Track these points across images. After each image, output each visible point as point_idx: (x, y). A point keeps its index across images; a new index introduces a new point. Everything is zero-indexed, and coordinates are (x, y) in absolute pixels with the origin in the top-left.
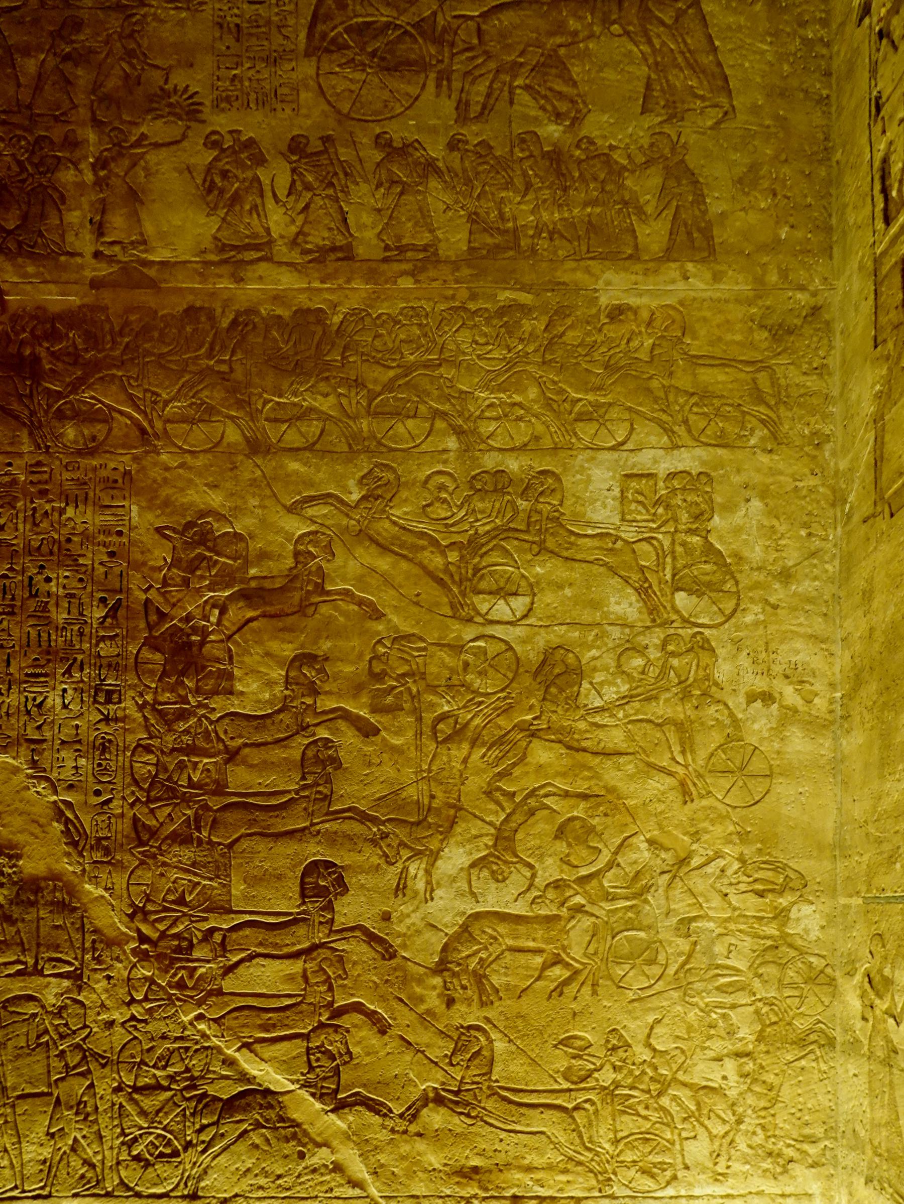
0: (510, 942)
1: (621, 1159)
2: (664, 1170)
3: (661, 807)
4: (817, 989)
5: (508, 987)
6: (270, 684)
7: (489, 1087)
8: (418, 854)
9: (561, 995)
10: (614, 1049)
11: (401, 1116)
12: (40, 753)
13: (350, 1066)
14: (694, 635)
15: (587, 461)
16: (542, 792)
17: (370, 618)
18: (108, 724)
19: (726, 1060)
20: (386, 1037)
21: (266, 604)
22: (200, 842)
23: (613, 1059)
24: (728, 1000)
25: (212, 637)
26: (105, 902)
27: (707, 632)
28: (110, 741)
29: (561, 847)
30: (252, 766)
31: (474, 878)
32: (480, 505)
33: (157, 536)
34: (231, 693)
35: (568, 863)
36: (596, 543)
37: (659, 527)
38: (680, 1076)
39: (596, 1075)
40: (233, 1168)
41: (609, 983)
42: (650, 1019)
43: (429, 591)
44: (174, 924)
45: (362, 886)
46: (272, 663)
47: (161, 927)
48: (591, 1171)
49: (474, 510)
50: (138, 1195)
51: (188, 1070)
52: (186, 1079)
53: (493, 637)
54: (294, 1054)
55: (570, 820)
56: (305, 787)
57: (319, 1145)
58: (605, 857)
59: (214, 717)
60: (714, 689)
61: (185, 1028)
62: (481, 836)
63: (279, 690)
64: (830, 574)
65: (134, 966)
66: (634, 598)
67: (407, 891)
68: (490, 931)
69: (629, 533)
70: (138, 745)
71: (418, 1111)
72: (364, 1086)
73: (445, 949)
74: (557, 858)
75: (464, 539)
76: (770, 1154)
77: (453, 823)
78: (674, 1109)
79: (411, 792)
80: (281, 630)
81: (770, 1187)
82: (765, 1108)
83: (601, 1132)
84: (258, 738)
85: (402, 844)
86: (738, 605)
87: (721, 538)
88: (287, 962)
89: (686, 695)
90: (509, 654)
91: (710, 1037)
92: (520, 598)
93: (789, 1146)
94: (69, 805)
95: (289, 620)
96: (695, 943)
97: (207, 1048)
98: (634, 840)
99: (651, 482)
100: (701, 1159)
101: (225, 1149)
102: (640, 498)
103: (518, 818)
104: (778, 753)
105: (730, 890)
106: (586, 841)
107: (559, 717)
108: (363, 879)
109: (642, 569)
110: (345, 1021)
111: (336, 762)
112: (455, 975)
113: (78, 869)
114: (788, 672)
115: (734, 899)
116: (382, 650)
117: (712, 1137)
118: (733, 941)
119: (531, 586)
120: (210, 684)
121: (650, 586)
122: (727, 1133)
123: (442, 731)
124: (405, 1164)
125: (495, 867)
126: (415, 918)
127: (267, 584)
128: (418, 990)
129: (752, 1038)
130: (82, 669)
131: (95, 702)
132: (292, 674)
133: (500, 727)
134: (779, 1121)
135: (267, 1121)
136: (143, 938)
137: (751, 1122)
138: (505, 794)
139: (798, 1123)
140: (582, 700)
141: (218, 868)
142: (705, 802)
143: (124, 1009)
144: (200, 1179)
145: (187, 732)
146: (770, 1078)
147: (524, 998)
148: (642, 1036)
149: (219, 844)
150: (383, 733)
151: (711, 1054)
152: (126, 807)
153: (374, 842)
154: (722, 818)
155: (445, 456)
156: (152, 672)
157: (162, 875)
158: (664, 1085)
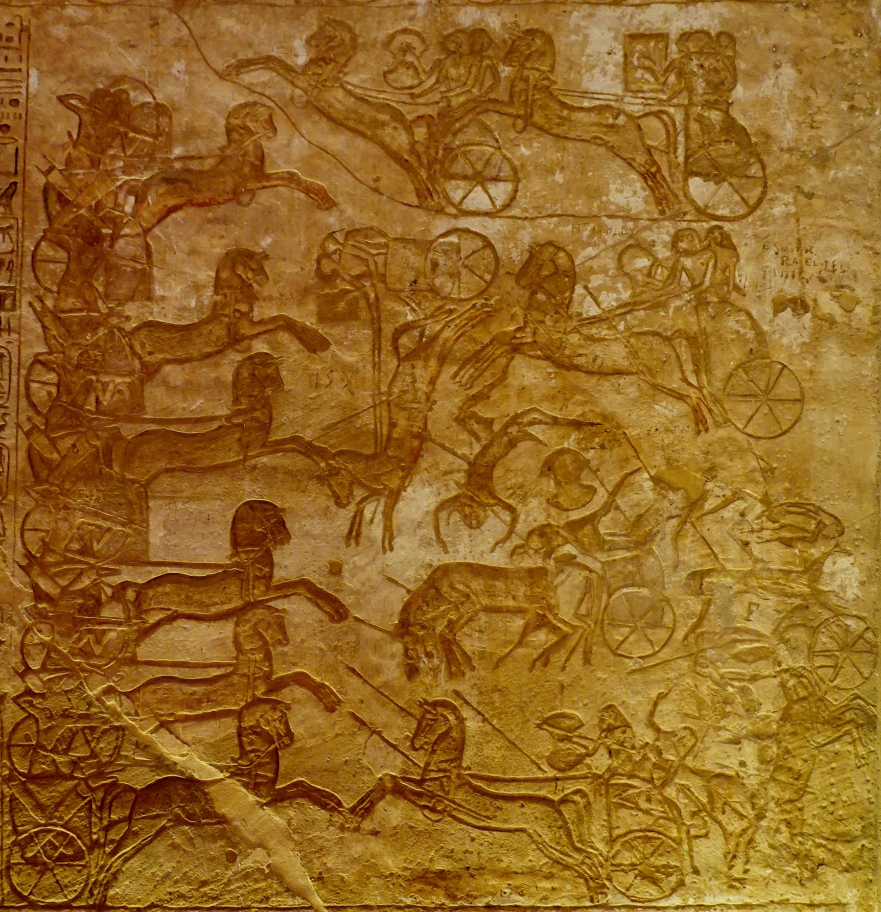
0: (485, 601)
1: (618, 861)
2: (669, 875)
3: (668, 439)
4: (855, 657)
5: (482, 655)
6: (197, 288)
7: (459, 776)
8: (373, 494)
9: (546, 664)
10: (610, 730)
11: (353, 810)
13: (292, 749)
14: (711, 230)
15: (584, 18)
16: (525, 420)
17: (319, 207)
19: (745, 743)
20: (335, 715)
23: (609, 742)
24: (747, 670)
25: (127, 231)
27: (727, 226)
29: (549, 485)
30: (175, 388)
31: (442, 524)
32: (453, 72)
34: (149, 299)
35: (557, 506)
36: (593, 118)
37: (670, 98)
38: (689, 762)
39: (588, 761)
40: (148, 873)
41: (605, 650)
42: (654, 694)
43: (392, 176)
45: (308, 534)
47: (63, 582)
48: (580, 876)
49: (446, 78)
50: (32, 905)
51: (94, 755)
52: (91, 766)
53: (467, 231)
54: (223, 735)
55: (562, 452)
56: (238, 413)
57: (254, 846)
58: (601, 497)
60: (734, 295)
61: (90, 705)
62: (451, 472)
63: (208, 294)
64: (876, 157)
66: (639, 184)
67: (362, 540)
68: (461, 587)
69: (635, 106)
71: (373, 804)
72: (307, 773)
73: (406, 608)
74: (543, 500)
75: (433, 111)
76: (796, 856)
77: (416, 456)
78: (682, 801)
79: (367, 420)
80: (210, 221)
81: (798, 896)
82: (791, 801)
83: (594, 829)
84: (180, 354)
85: (355, 481)
86: (764, 193)
87: (744, 112)
88: (215, 625)
89: (701, 303)
90: (488, 252)
91: (725, 715)
92: (501, 185)
93: (820, 845)
95: (220, 211)
96: (709, 603)
97: (117, 729)
98: (637, 478)
99: (661, 46)
100: (712, 861)
101: (138, 850)
102: (647, 63)
103: (495, 450)
104: (811, 373)
105: (753, 538)
106: (578, 478)
107: (549, 329)
108: (307, 524)
109: (649, 150)
110: (286, 695)
111: (276, 381)
112: (418, 640)
114: (824, 275)
115: (756, 550)
116: (332, 247)
117: (727, 835)
118: (755, 600)
119: (515, 170)
121: (659, 170)
122: (744, 831)
123: (404, 346)
124: (357, 868)
125: (467, 510)
126: (372, 573)
127: (194, 165)
128: (374, 659)
129: (777, 716)
132: (224, 275)
133: (474, 340)
134: (807, 815)
135: (190, 816)
137: (773, 816)
138: (480, 420)
139: (831, 817)
140: (575, 309)
142: (721, 433)
143: (18, 682)
144: (108, 886)
146: (798, 764)
147: (501, 669)
148: (643, 715)
149: (133, 482)
150: (333, 347)
151: (727, 735)
153: (321, 479)
154: (742, 451)
155: (411, 12)
158: (669, 772)
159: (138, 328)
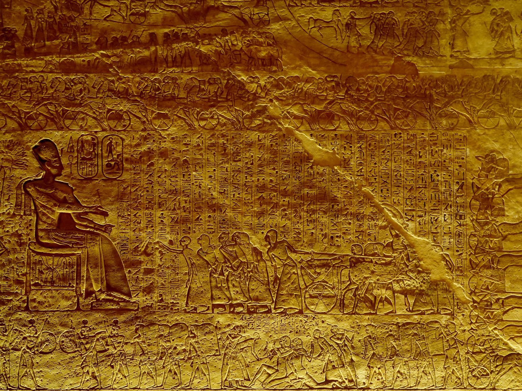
12: (437, 237)
18: (460, 227)
21: (516, 183)
22: (494, 268)
25: (496, 196)
26: (461, 289)
28: (461, 233)
33: (476, 160)
34: (504, 216)
44: (485, 296)
46: (519, 205)
59: (497, 224)
65: (472, 311)
70: (471, 234)
84: (514, 232)
94: (447, 255)
113: (451, 278)
120: (496, 213)
127: (516, 177)
130: (451, 207)
131: (456, 219)
136: (474, 302)
141: (500, 277)
145: (488, 230)
152: (468, 256)
156: (475, 208)
157: (480, 280)
159: (500, 224)
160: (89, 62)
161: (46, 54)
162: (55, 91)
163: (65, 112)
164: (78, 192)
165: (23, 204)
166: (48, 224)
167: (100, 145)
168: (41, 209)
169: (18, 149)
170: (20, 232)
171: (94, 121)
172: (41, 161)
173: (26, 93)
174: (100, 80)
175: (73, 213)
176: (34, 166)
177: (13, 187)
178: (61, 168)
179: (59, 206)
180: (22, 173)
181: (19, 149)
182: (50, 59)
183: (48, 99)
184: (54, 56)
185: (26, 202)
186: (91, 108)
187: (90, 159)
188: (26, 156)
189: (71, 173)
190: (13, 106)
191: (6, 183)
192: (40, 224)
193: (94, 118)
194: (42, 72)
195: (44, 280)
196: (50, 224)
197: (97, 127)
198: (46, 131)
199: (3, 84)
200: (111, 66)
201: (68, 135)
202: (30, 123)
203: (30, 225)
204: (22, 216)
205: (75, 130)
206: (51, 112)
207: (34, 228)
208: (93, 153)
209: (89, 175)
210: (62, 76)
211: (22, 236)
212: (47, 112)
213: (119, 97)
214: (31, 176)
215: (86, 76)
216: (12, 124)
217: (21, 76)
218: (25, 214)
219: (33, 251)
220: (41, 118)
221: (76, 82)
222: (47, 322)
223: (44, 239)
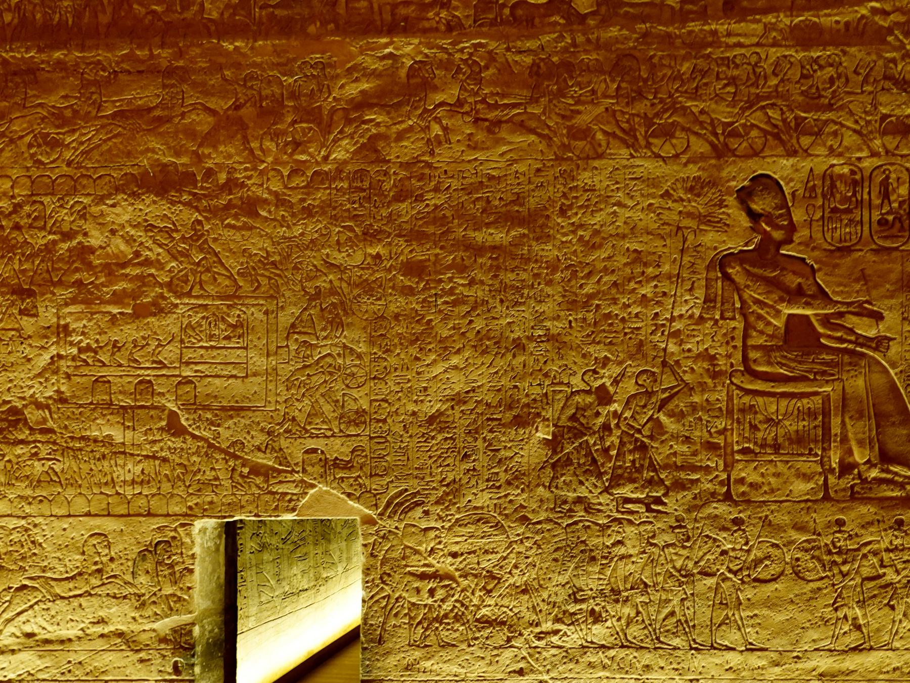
160: (847, 24)
161: (765, 11)
162: (782, 80)
163: (799, 121)
164: (826, 274)
165: (719, 298)
166: (768, 335)
167: (866, 184)
168: (754, 308)
169: (711, 194)
170: (712, 352)
171: (855, 137)
172: (754, 216)
173: (726, 86)
174: (869, 59)
175: (816, 315)
176: (740, 226)
177: (701, 266)
178: (792, 228)
179: (789, 302)
180: (719, 239)
181: (714, 194)
182: (774, 20)
183: (768, 98)
184: (782, 15)
185: (726, 294)
186: (851, 113)
187: (848, 211)
188: (726, 206)
189: (811, 237)
190: (702, 112)
191: (686, 259)
192: (751, 337)
193: (855, 131)
194: (758, 44)
195: (759, 442)
196: (772, 337)
197: (860, 150)
198: (764, 158)
199: (683, 69)
200: (890, 31)
201: (807, 164)
202: (734, 143)
203: (733, 338)
204: (716, 322)
205: (818, 156)
206: (773, 121)
207: (739, 344)
208: (854, 199)
209: (845, 241)
210: (797, 51)
211: (716, 359)
212: (766, 123)
213: (905, 91)
214: (734, 245)
215: (842, 51)
216: (700, 147)
217: (718, 53)
218: (722, 317)
219: (739, 388)
220: (754, 133)
221: (822, 62)
222: (766, 522)
223: (760, 365)
